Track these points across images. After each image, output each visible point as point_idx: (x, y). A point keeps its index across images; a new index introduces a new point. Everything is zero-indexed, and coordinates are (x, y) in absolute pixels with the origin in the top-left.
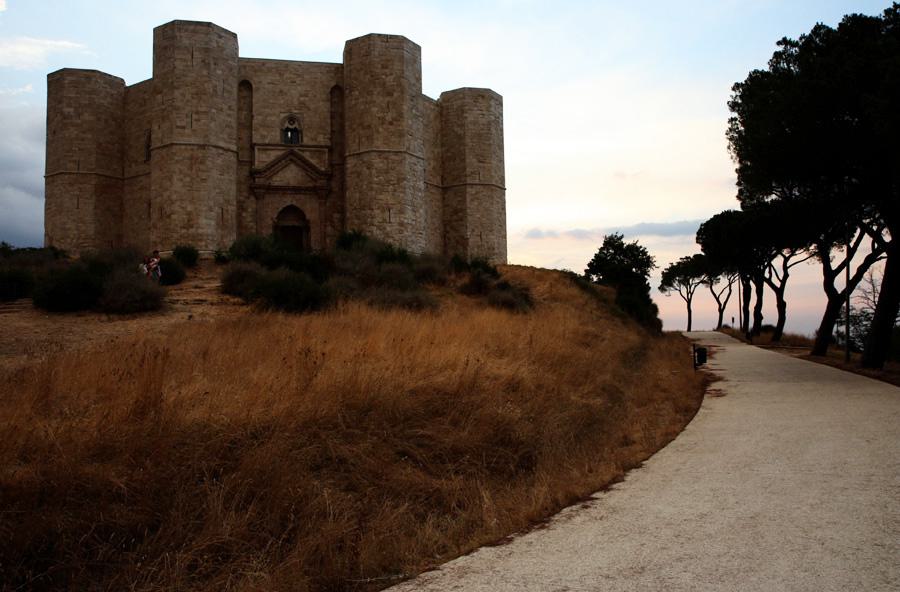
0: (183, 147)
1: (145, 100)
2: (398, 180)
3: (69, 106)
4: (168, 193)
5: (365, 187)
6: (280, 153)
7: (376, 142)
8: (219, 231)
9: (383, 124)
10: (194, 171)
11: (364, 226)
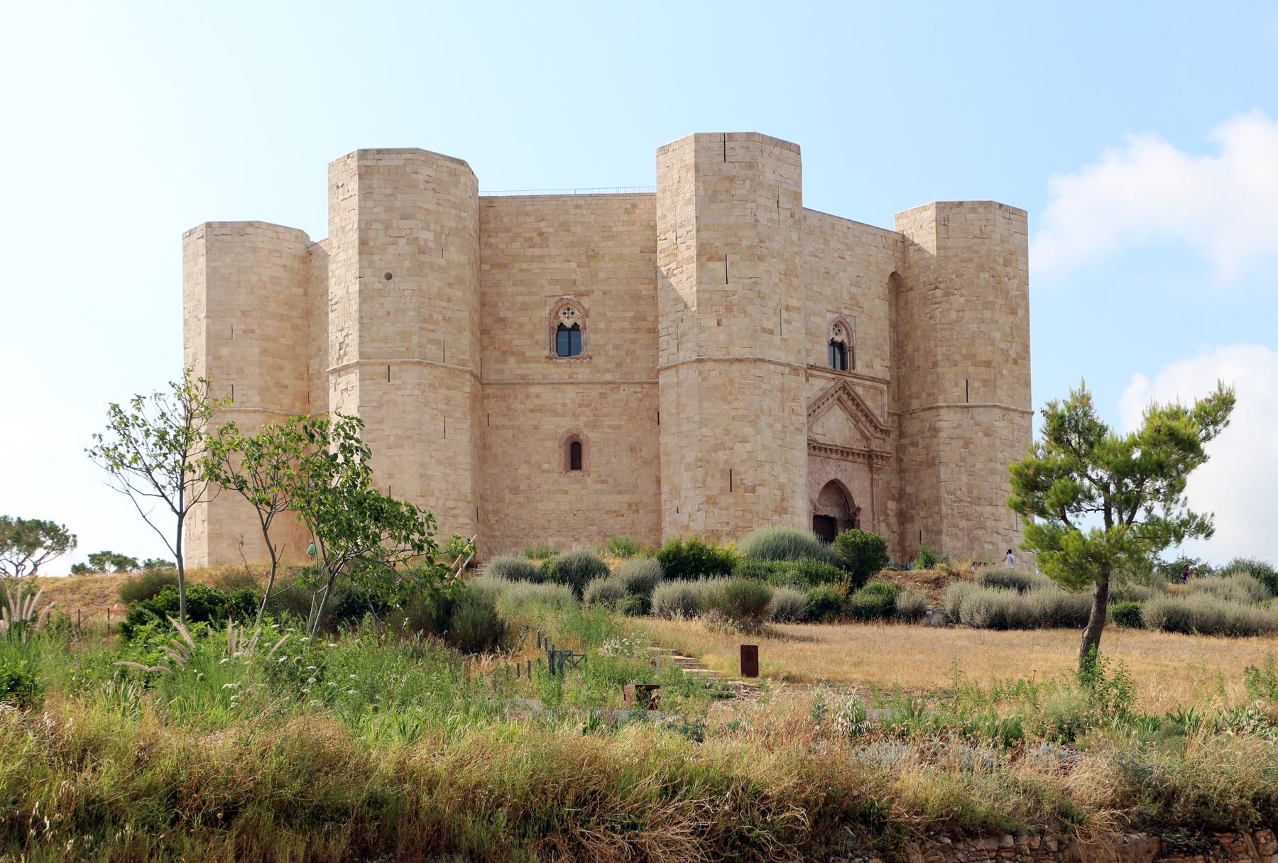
0: (772, 367)
1: (541, 234)
3: (428, 230)
4: (748, 447)
5: (978, 466)
7: (998, 391)
9: (1007, 361)
10: (786, 411)
11: (979, 533)
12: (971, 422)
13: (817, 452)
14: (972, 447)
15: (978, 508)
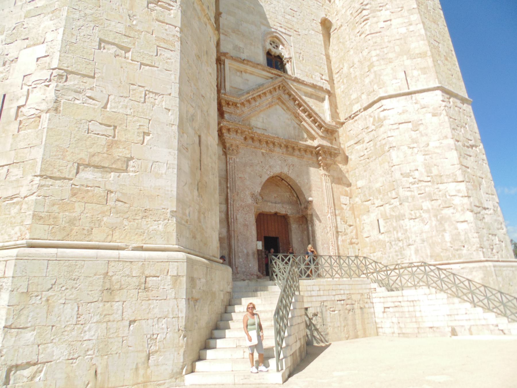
2: (475, 141)
4: (40, 50)
5: (432, 145)
6: (260, 81)
8: (196, 193)
12: (417, 106)
13: (257, 144)
14: (421, 128)
15: (441, 186)
